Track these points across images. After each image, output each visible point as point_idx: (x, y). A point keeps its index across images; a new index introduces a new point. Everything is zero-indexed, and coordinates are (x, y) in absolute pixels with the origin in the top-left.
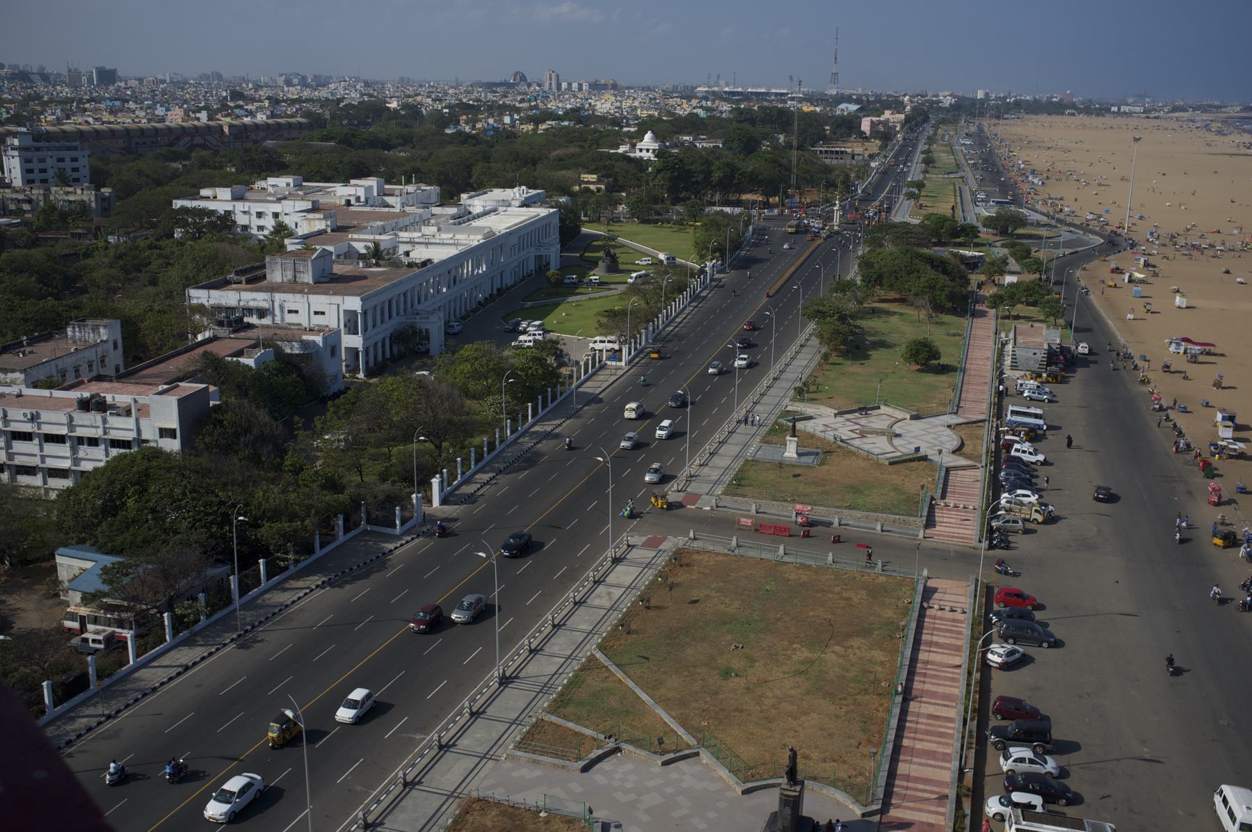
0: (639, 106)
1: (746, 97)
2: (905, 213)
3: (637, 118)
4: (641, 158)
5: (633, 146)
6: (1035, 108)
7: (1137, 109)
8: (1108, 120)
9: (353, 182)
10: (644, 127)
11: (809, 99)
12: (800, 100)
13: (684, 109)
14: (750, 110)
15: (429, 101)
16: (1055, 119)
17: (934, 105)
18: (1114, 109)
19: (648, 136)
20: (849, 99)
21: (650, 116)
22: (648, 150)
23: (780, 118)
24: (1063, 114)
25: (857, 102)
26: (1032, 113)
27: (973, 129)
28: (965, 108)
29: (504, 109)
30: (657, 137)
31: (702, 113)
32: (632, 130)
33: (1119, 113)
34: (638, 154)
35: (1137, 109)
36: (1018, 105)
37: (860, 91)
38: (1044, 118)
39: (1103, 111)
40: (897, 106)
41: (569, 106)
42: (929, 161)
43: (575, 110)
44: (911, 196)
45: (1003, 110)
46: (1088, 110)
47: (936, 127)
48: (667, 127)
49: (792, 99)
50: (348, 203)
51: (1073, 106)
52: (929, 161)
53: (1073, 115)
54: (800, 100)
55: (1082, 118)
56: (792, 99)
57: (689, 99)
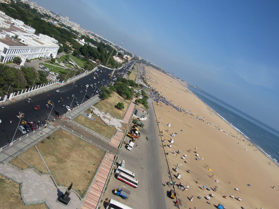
0: (83, 32)
1: (104, 41)
2: (125, 77)
3: (81, 34)
4: (80, 43)
5: (79, 40)
6: (154, 67)
7: (171, 75)
8: (166, 75)
9: (16, 20)
10: (83, 37)
11: (116, 47)
12: (114, 46)
13: (91, 37)
14: (104, 44)
15: (40, 10)
16: (157, 70)
17: (138, 59)
18: (168, 73)
19: (83, 40)
20: (122, 50)
21: (84, 36)
22: (82, 42)
23: (109, 48)
24: (159, 70)
25: (124, 51)
26: (154, 68)
27: (142, 66)
28: (143, 62)
29: (55, 20)
30: (85, 41)
31: (94, 39)
32: (80, 37)
33: (168, 75)
34: (79, 42)
35: (171, 75)
36: (152, 65)
37: (126, 50)
38: (154, 70)
39: (166, 73)
40: (131, 56)
41: (69, 26)
42: (133, 68)
43: (70, 27)
44: (128, 74)
45: (148, 65)
46: (163, 72)
47: (136, 63)
48: (88, 39)
49: (113, 45)
50: (14, 24)
51: (161, 70)
52: (133, 68)
53: (160, 71)
54: (114, 46)
55: (161, 72)
56: (113, 45)
57: (93, 36)
